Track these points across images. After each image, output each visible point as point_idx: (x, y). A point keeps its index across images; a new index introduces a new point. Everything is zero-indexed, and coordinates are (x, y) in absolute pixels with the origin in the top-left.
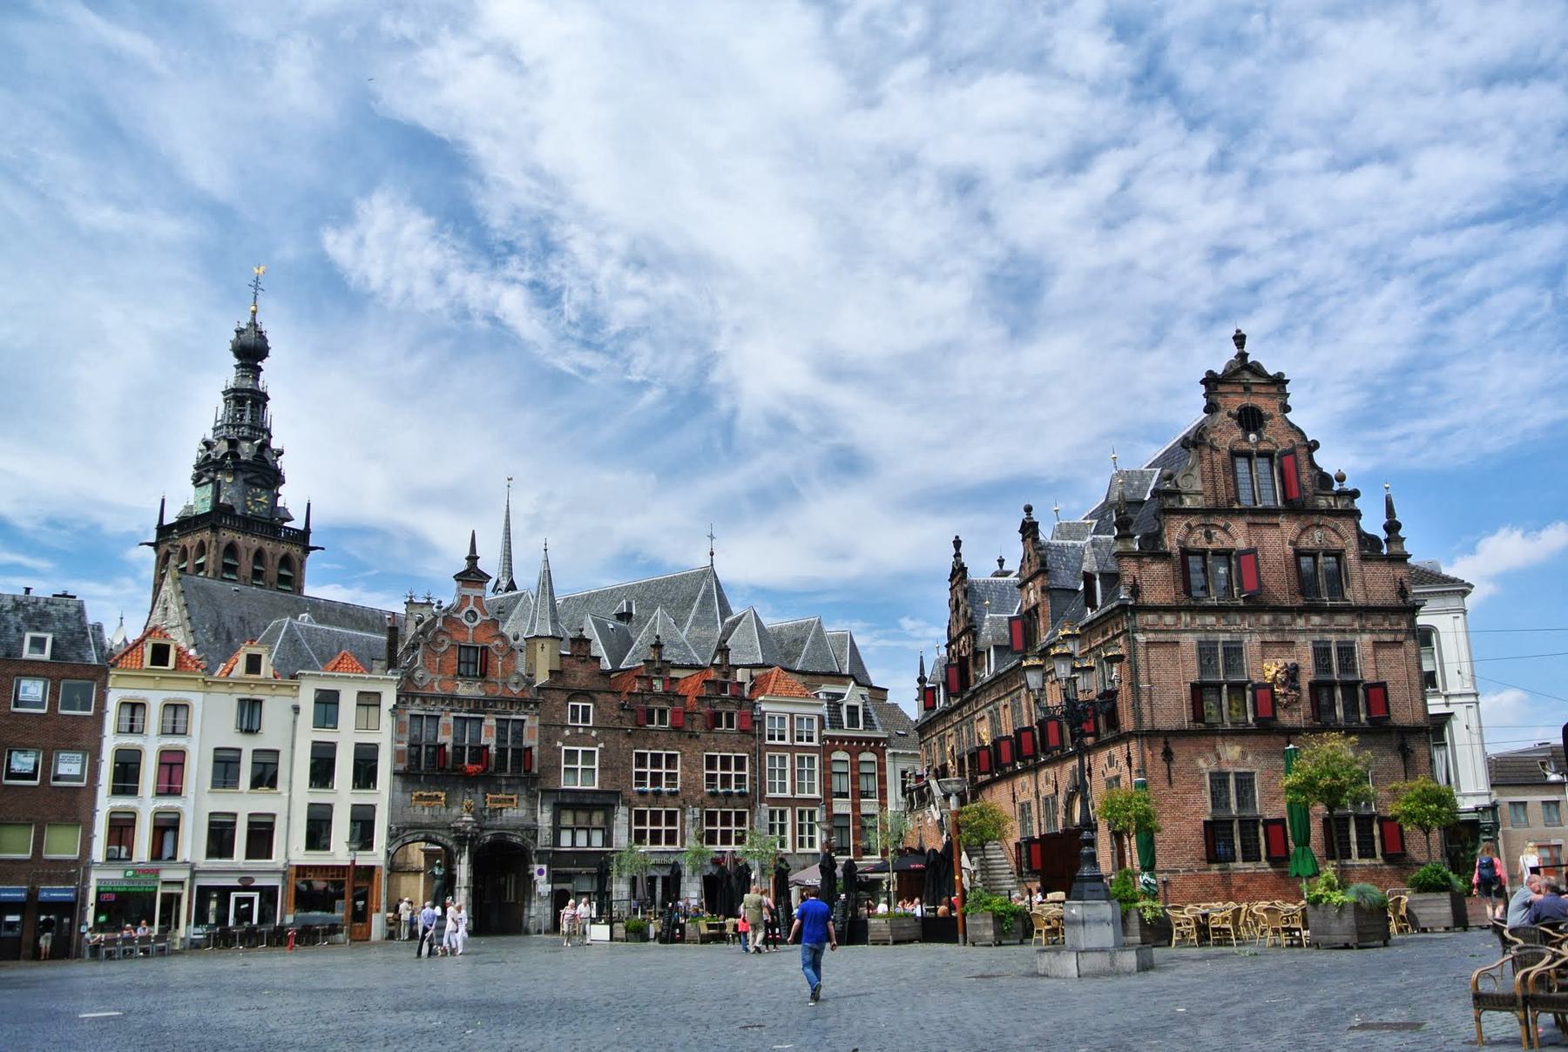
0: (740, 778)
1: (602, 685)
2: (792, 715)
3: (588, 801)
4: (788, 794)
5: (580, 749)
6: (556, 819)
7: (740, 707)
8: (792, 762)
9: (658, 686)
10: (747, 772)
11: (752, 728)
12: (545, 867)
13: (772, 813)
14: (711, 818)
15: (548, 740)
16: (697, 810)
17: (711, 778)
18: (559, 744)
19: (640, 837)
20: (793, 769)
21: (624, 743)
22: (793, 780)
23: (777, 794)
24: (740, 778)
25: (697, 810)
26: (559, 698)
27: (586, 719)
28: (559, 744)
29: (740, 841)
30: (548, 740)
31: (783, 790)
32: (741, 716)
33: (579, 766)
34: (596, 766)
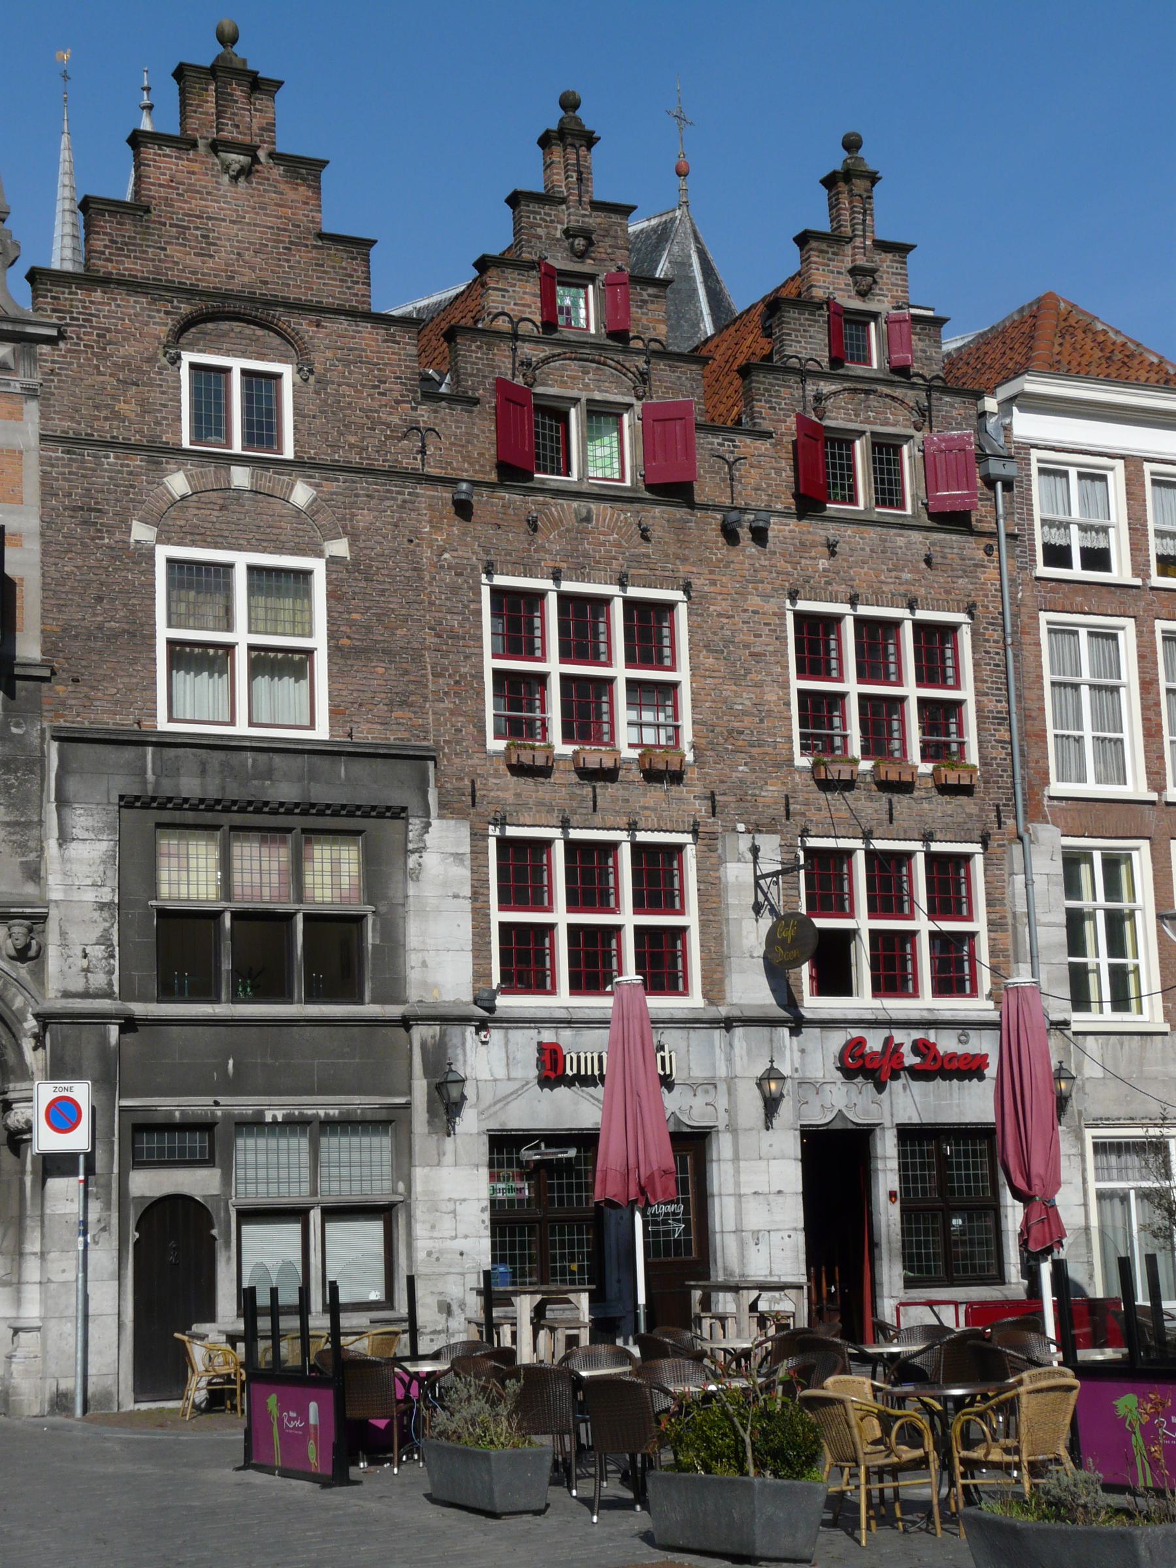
0: (940, 716)
1: (329, 291)
2: (1134, 463)
3: (286, 792)
4: (1136, 787)
5: (241, 560)
6: (136, 867)
7: (925, 415)
8: (1146, 657)
9: (584, 311)
10: (967, 693)
11: (971, 499)
12: (81, 1092)
13: (1073, 861)
14: (826, 871)
15: (87, 512)
16: (770, 845)
17: (819, 710)
18: (141, 532)
19: (524, 958)
20: (1148, 685)
21: (441, 539)
22: (1152, 732)
23: (1090, 788)
24: (940, 716)
25: (770, 845)
26: (142, 322)
27: (262, 427)
28: (141, 532)
29: (952, 977)
30: (87, 512)
31: (1115, 771)
32: (928, 461)
33: (241, 637)
34: (319, 642)
